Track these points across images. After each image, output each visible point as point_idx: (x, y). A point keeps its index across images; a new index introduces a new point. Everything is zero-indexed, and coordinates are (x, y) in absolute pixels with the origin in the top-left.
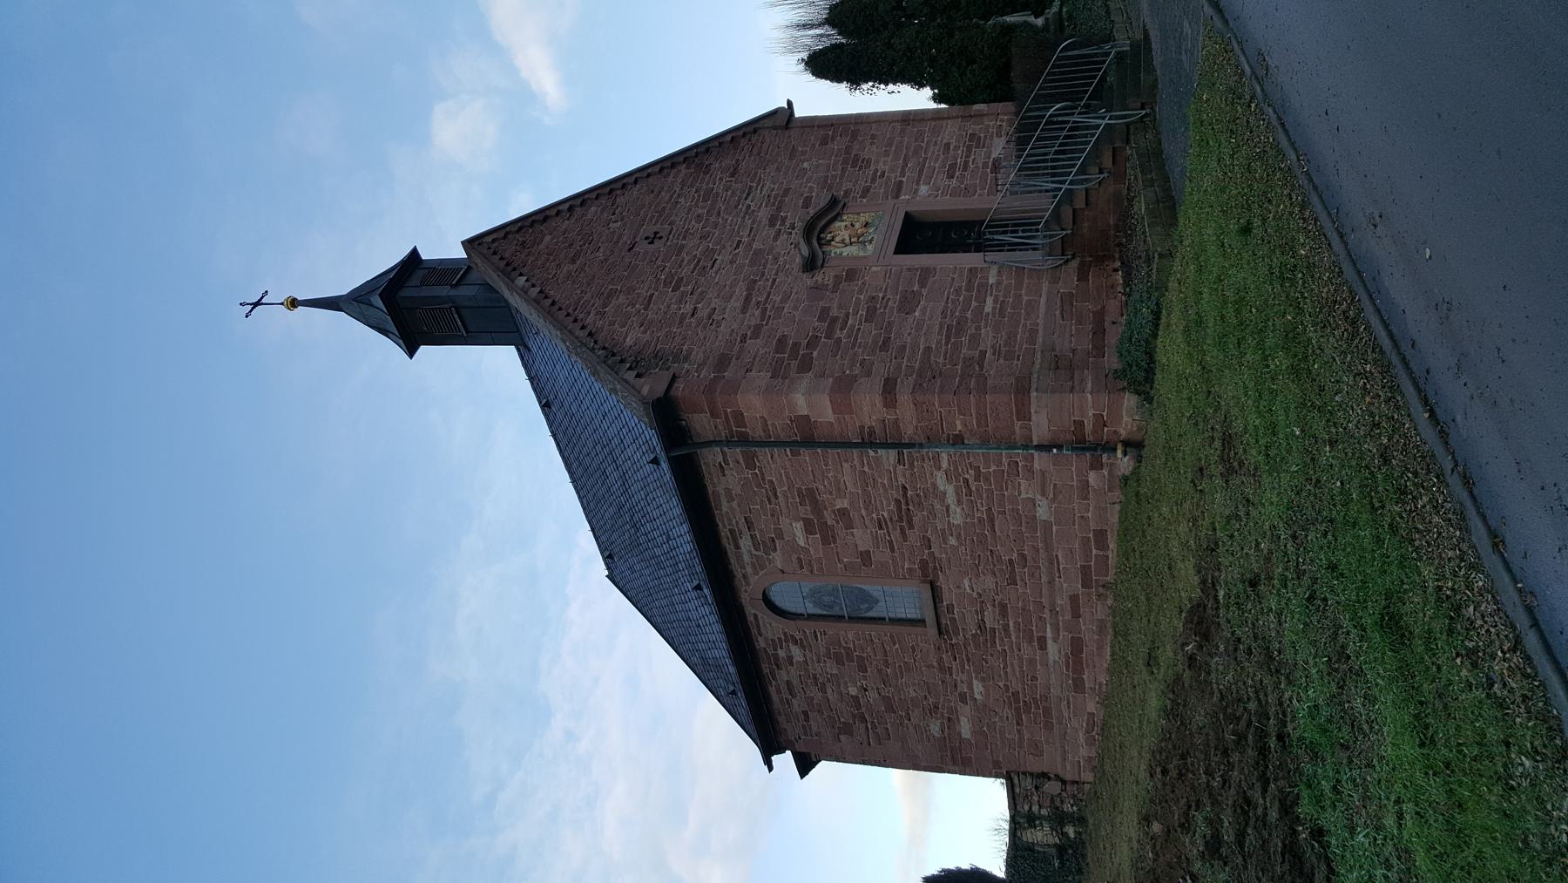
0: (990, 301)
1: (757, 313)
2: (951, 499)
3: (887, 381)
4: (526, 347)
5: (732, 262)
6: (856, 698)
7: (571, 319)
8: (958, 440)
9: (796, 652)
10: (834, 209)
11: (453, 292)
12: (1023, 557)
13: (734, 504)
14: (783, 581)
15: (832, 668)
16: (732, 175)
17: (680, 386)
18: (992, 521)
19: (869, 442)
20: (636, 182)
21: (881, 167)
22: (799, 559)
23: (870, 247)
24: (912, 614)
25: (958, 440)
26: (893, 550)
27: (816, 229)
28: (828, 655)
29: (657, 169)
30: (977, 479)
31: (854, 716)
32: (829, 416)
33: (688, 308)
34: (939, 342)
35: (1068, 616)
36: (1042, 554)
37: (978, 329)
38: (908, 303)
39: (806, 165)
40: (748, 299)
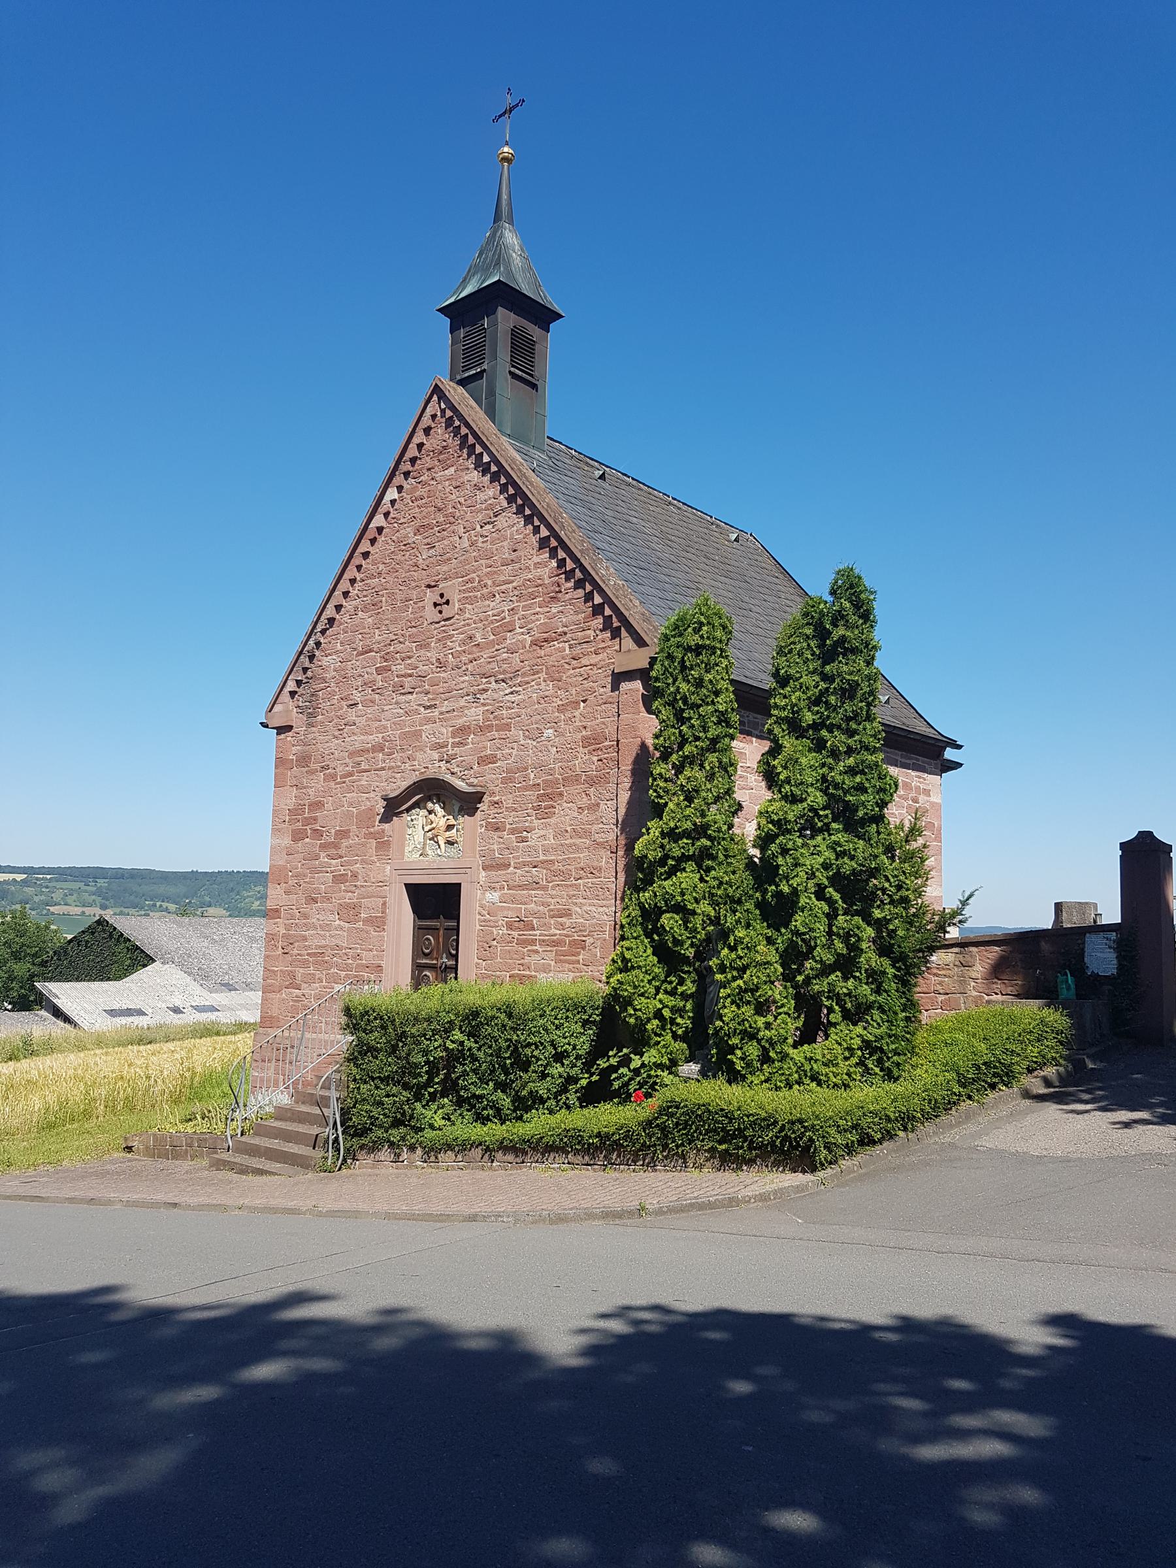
23: (416, 856)
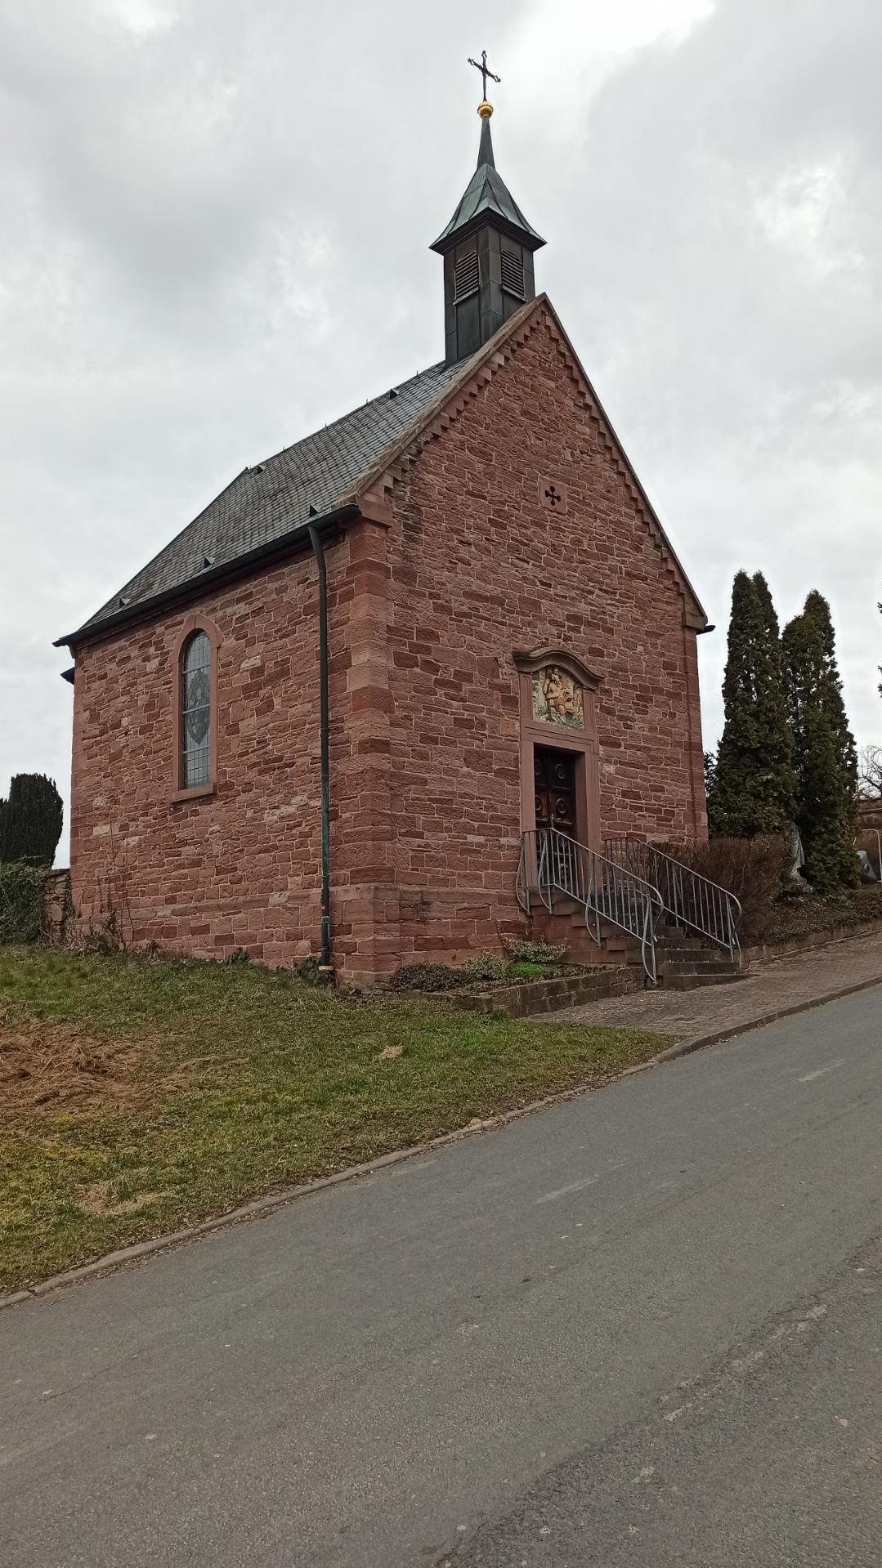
0: (481, 839)
1: (465, 608)
2: (285, 810)
3: (387, 743)
4: (445, 369)
5: (524, 579)
6: (118, 725)
7: (454, 416)
8: (331, 815)
9: (153, 664)
10: (588, 681)
11: (494, 288)
12: (239, 881)
13: (274, 596)
14: (217, 644)
15: (143, 700)
16: (628, 573)
17: (378, 533)
18: (267, 851)
19: (328, 727)
20: (620, 474)
21: (637, 725)
22: (229, 664)
23: (543, 718)
24: (191, 776)
25: (331, 815)
26: (241, 755)
27: (561, 662)
28: (153, 696)
29: (635, 495)
30: (302, 835)
31: (105, 724)
32: (351, 688)
33: (470, 536)
34: (431, 792)
35: (193, 924)
36: (241, 899)
37: (448, 829)
38: (475, 759)
39: (640, 649)
40: (480, 597)
